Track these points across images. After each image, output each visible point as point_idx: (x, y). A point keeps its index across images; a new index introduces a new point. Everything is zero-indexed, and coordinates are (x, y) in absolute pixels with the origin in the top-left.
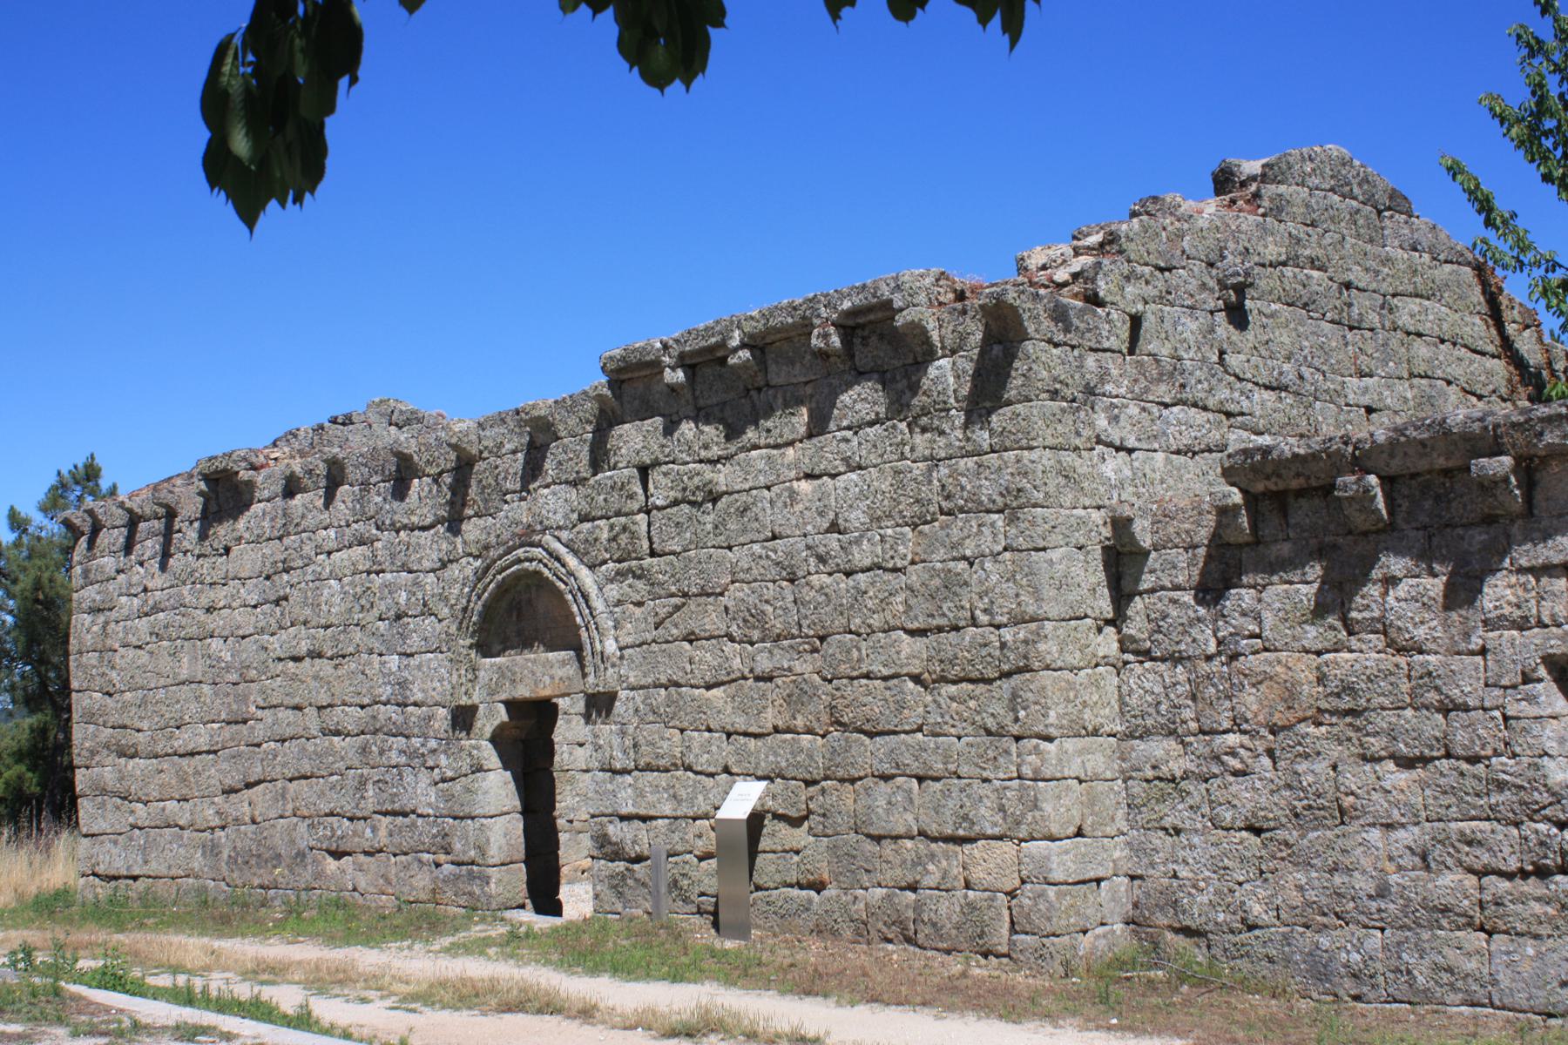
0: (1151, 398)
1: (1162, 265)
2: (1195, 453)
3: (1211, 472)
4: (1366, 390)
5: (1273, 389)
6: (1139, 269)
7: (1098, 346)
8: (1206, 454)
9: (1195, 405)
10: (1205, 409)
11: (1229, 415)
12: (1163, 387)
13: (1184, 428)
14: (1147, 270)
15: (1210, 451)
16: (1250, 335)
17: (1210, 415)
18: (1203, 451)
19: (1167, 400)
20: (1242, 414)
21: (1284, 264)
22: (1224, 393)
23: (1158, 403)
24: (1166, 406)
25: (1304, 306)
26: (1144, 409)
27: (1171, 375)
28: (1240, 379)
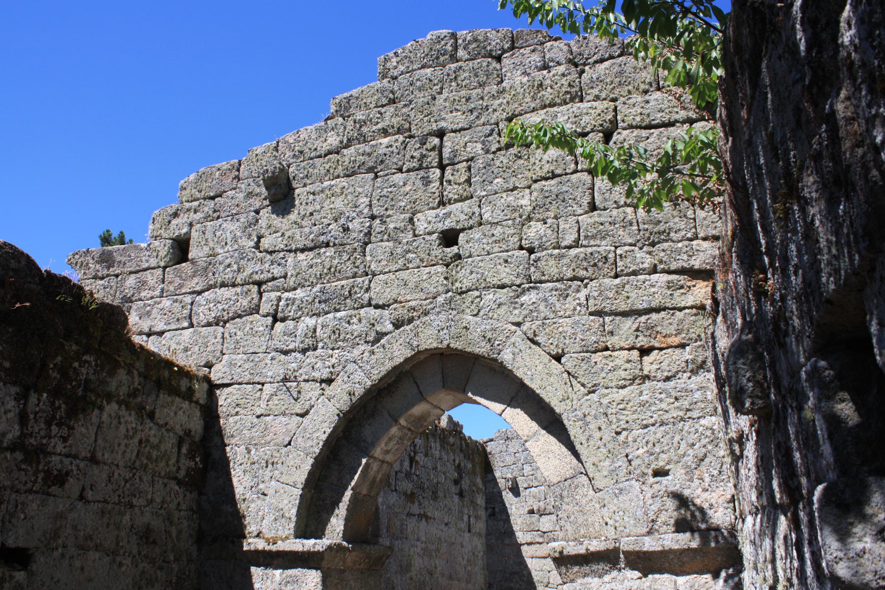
0: (183, 291)
1: (212, 194)
2: (225, 322)
3: (239, 333)
4: (448, 215)
5: (311, 249)
6: (187, 205)
7: (137, 268)
8: (237, 320)
9: (223, 285)
10: (234, 285)
11: (259, 284)
12: (196, 280)
13: (211, 305)
14: (196, 203)
15: (240, 316)
16: (293, 217)
17: (239, 289)
18: (233, 318)
19: (198, 288)
20: (274, 279)
21: (346, 147)
22: (250, 268)
23: (190, 293)
24: (199, 293)
25: (370, 170)
26: (176, 301)
27: (206, 269)
28: (271, 253)
